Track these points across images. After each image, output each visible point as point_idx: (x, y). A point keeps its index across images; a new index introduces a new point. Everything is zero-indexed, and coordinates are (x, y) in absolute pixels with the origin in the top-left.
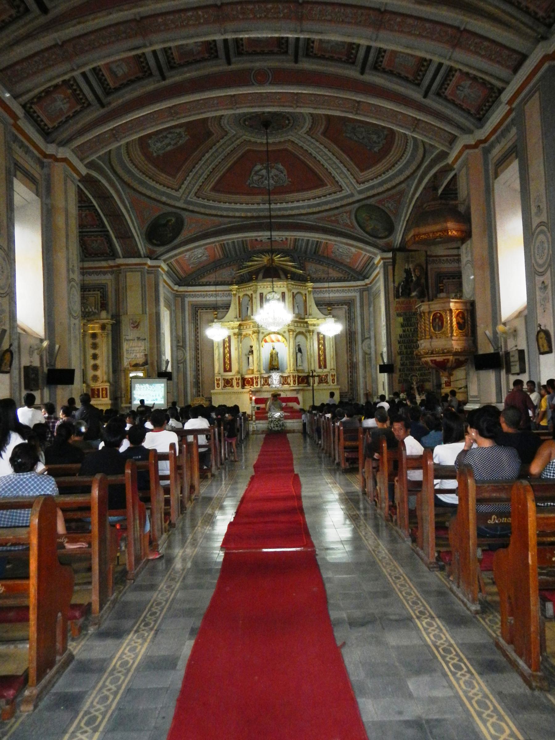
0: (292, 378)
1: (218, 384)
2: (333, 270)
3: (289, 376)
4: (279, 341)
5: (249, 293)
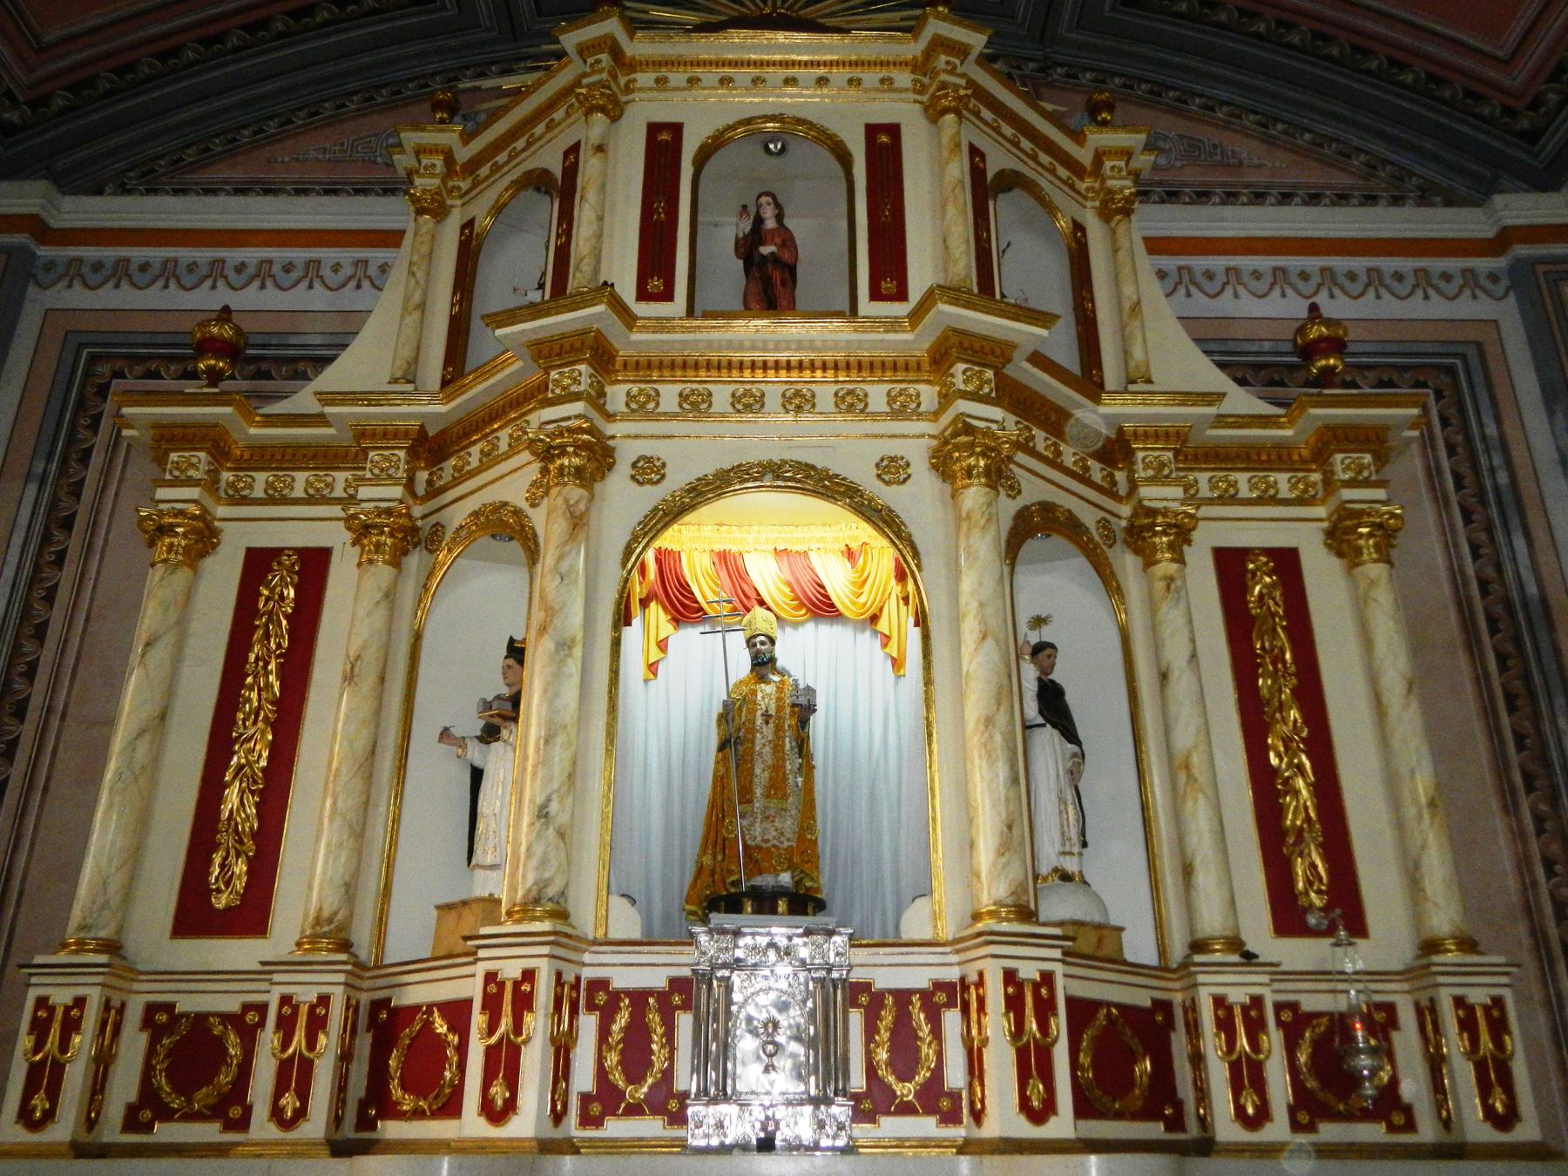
0: (996, 1023)
2: (1270, 141)
3: (959, 994)
4: (821, 607)
5: (550, 159)
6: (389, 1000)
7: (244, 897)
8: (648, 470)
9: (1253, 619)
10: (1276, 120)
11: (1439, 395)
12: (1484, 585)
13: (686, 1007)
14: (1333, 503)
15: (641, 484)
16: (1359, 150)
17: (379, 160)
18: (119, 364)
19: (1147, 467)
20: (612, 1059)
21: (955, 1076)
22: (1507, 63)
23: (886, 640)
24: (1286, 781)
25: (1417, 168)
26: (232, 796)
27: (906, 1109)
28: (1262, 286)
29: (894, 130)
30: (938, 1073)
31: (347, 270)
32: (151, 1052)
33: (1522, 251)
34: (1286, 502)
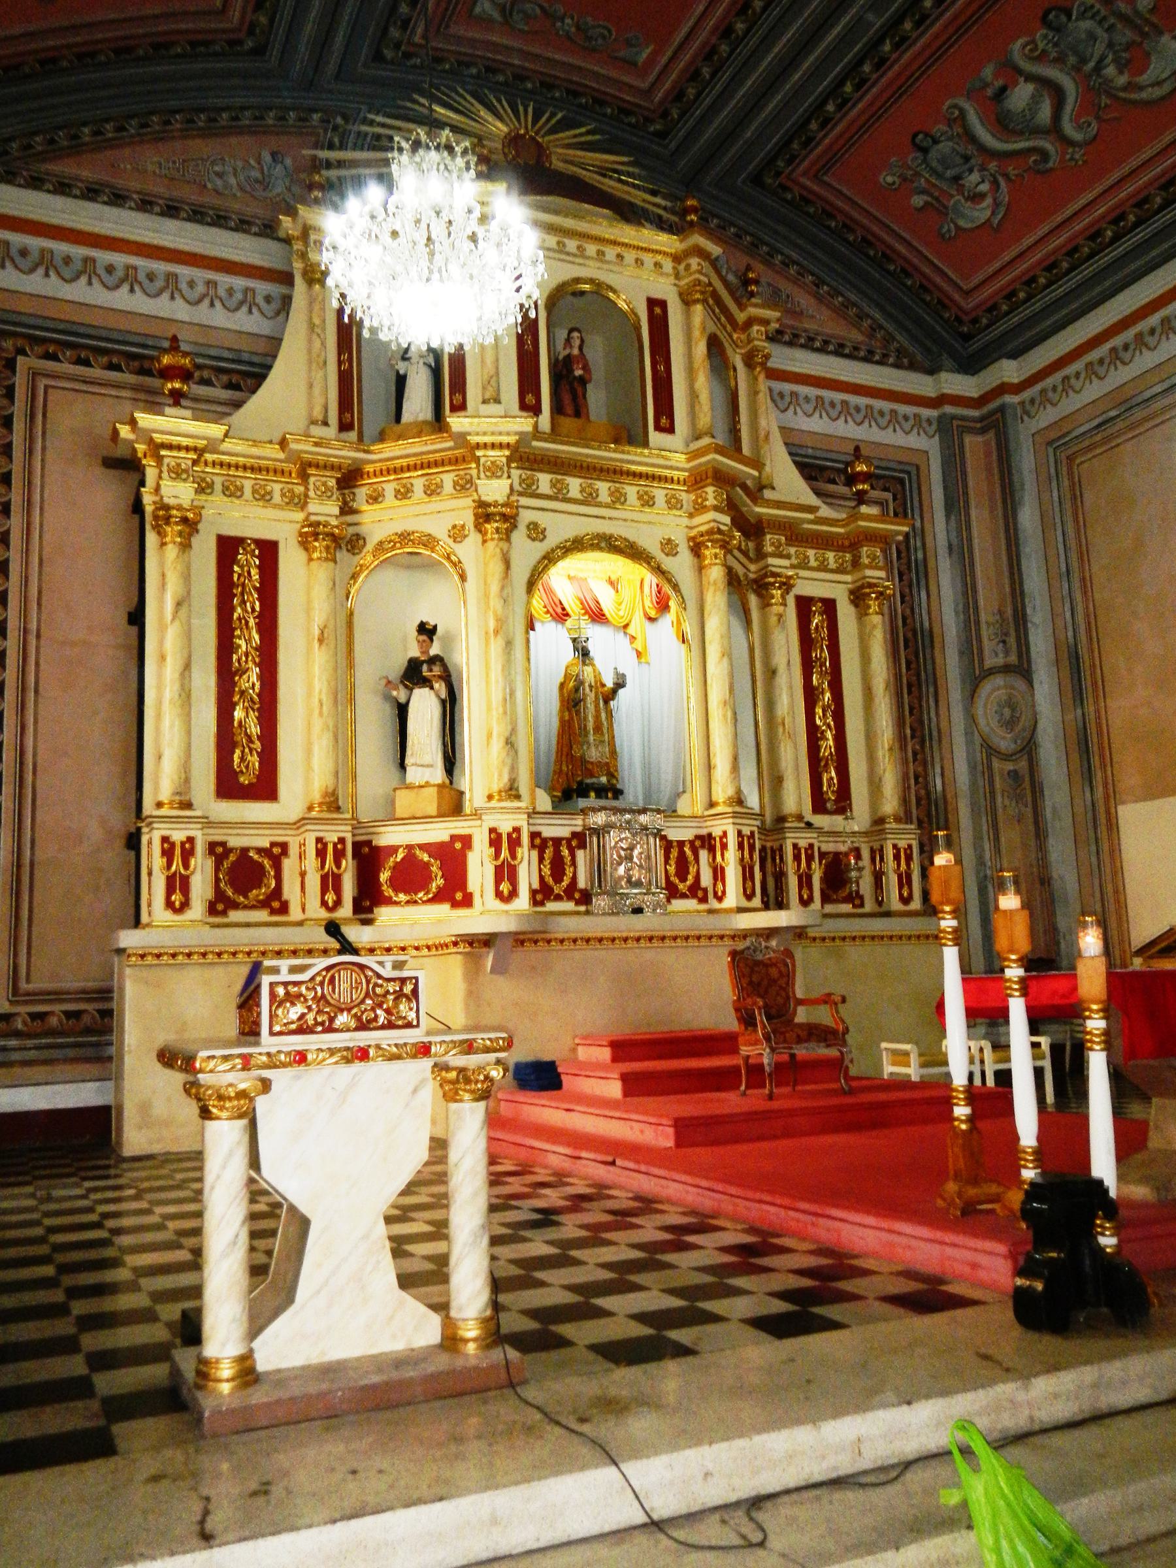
1: (178, 885)
2: (820, 299)
4: (597, 616)
6: (370, 842)
7: (258, 777)
8: (536, 532)
9: (812, 640)
10: (824, 283)
11: (895, 499)
12: (904, 619)
13: (582, 845)
14: (858, 575)
15: (534, 540)
16: (868, 316)
17: (209, 186)
18: (20, 342)
19: (772, 544)
20: (547, 871)
21: (706, 880)
22: (968, 293)
23: (633, 638)
24: (823, 732)
25: (899, 337)
26: (238, 714)
27: (684, 896)
28: (809, 408)
29: (663, 304)
30: (697, 877)
31: (201, 289)
32: (217, 870)
33: (949, 409)
34: (832, 571)
